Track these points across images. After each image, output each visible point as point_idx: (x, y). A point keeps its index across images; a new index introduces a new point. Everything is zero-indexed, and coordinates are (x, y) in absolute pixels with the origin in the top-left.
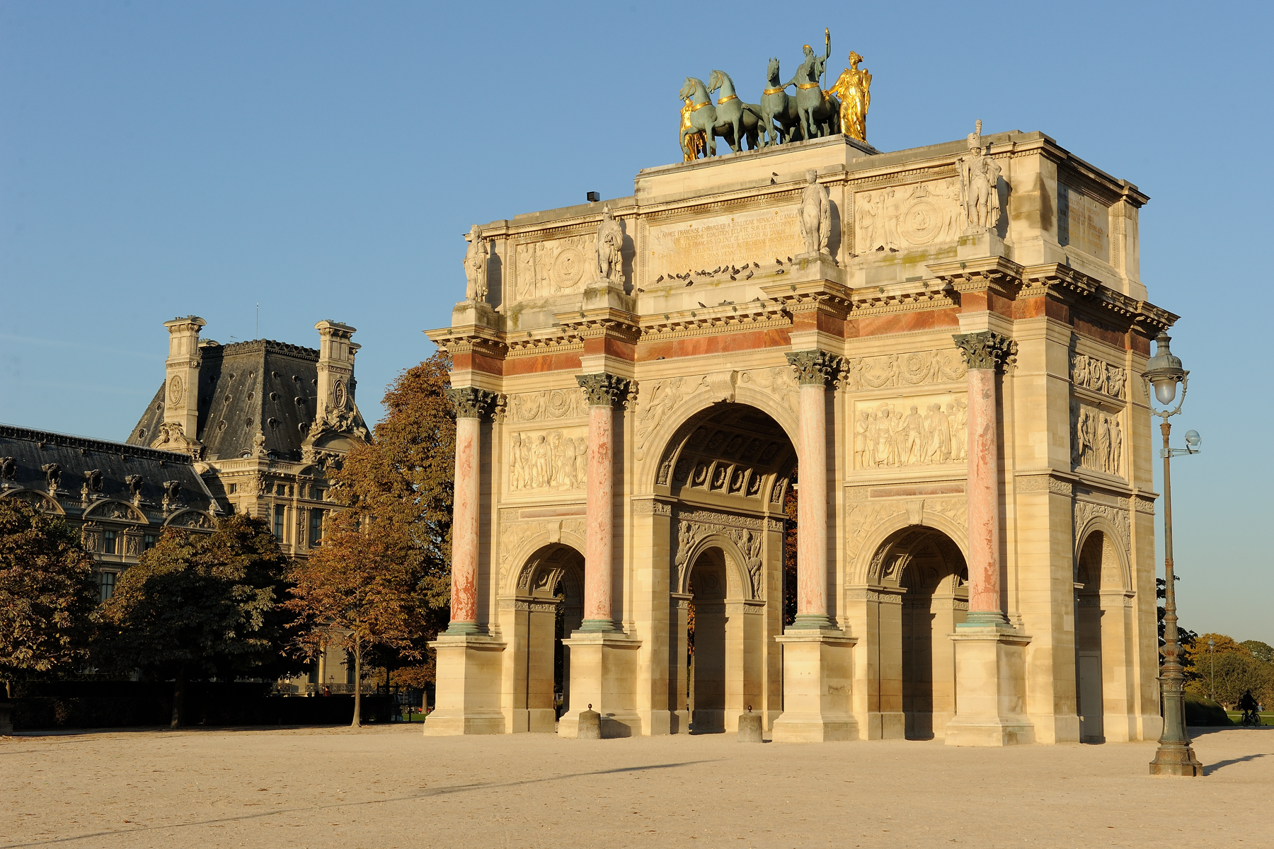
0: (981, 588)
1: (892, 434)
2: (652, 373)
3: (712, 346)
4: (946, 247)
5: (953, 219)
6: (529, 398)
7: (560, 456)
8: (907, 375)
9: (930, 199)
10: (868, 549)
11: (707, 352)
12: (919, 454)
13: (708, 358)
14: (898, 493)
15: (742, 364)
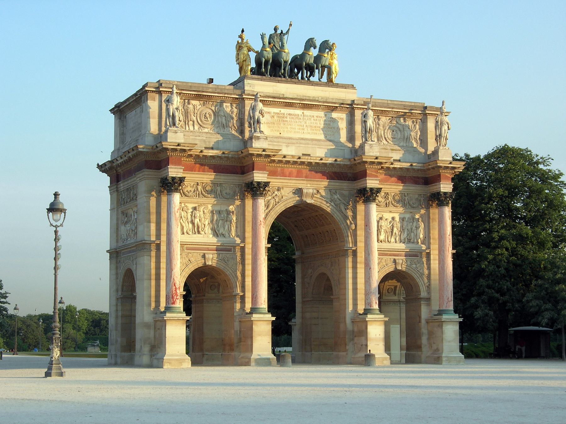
3: (299, 175)
7: (207, 219)
11: (296, 177)
14: (390, 255)
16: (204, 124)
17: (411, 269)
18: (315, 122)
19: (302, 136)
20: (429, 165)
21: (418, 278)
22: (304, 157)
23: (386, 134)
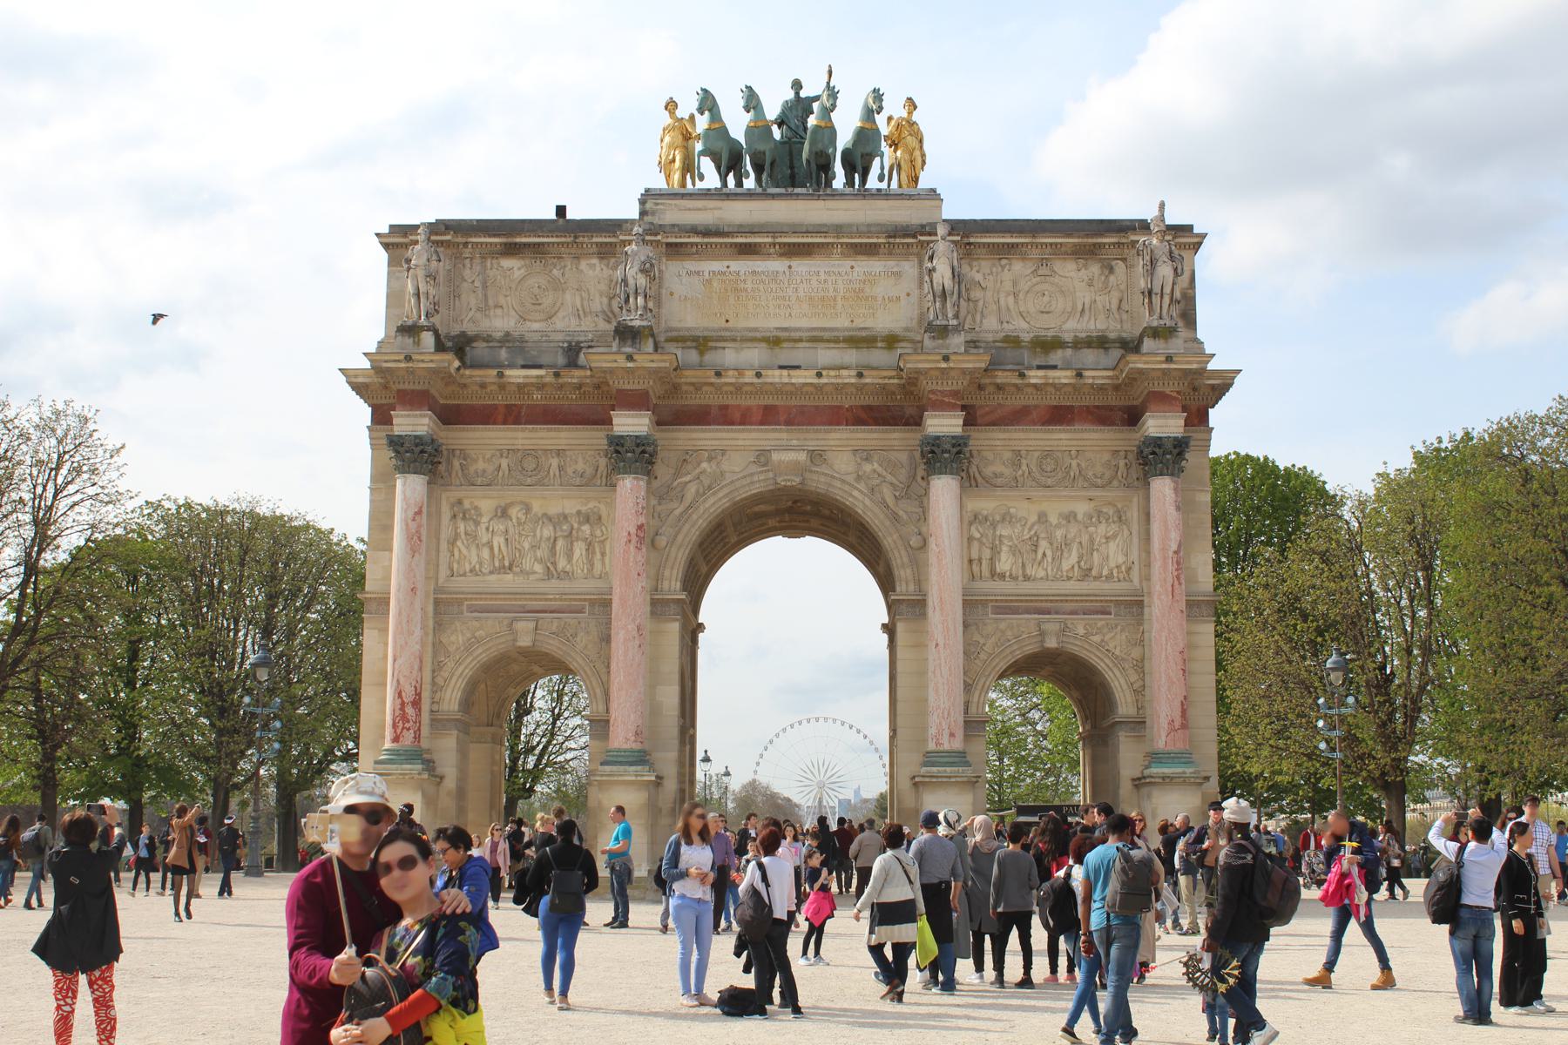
0: (1177, 724)
1: (1016, 542)
2: (680, 442)
3: (767, 416)
4: (1083, 335)
5: (1087, 306)
6: (480, 456)
7: (528, 536)
8: (1037, 475)
10: (989, 675)
11: (762, 423)
12: (1050, 568)
13: (766, 431)
14: (1028, 611)
15: (814, 443)
17: (1086, 646)
21: (1111, 669)
22: (770, 372)
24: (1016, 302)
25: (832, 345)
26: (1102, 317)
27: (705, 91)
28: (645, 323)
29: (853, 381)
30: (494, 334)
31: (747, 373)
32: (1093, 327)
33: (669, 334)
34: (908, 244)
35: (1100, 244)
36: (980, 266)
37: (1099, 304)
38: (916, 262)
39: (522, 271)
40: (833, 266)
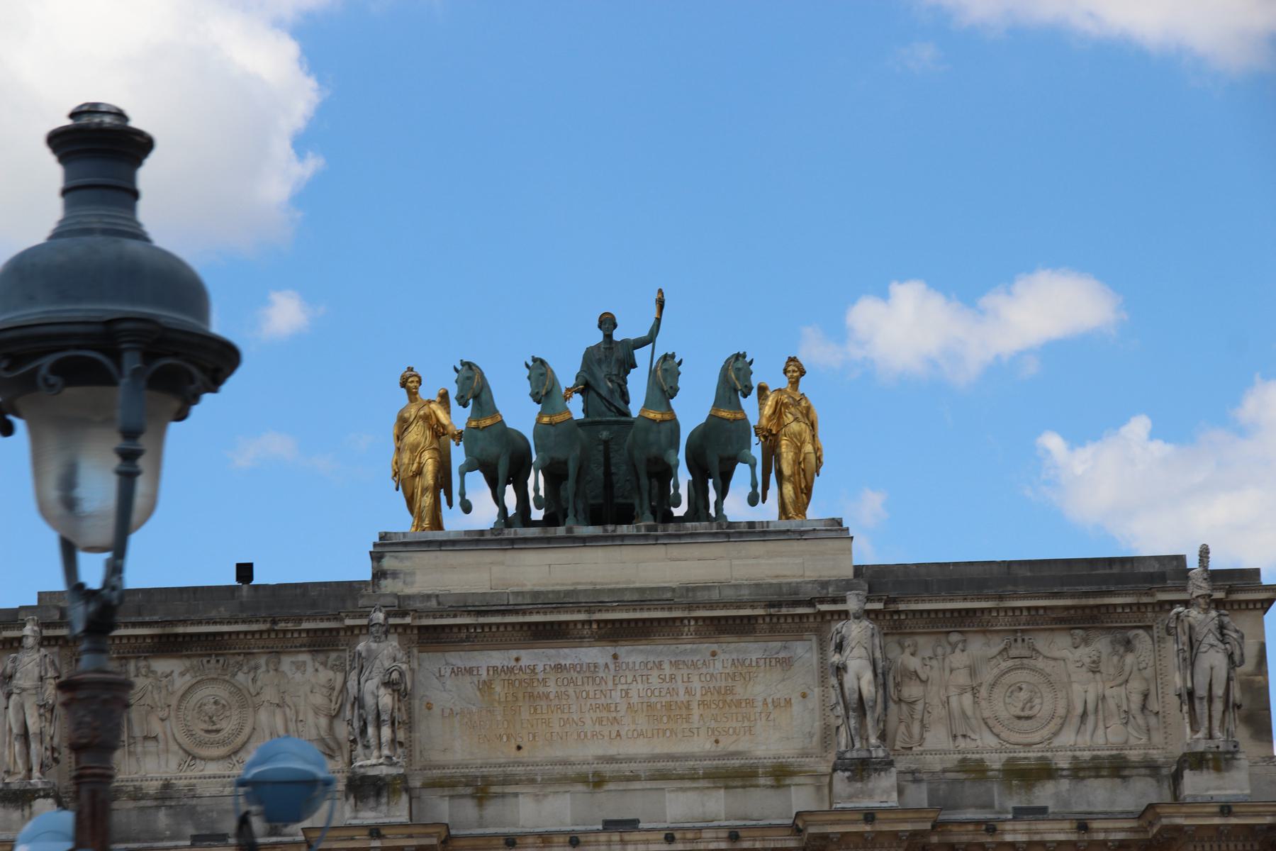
4: (1087, 755)
5: (1091, 707)
9: (1040, 663)
16: (201, 744)
18: (665, 685)
19: (612, 751)
20: (1151, 824)
22: (592, 838)
23: (984, 704)
24: (976, 703)
25: (688, 784)
26: (1115, 724)
27: (469, 365)
28: (393, 771)
29: (723, 845)
30: (145, 784)
31: (556, 839)
32: (1100, 740)
33: (429, 773)
34: (801, 616)
35: (1107, 606)
36: (916, 645)
37: (1111, 704)
38: (815, 646)
39: (188, 677)
40: (684, 652)
